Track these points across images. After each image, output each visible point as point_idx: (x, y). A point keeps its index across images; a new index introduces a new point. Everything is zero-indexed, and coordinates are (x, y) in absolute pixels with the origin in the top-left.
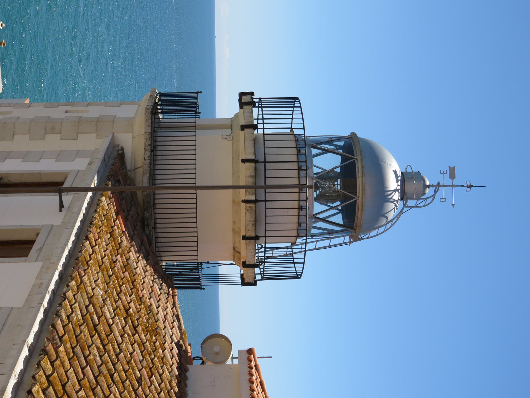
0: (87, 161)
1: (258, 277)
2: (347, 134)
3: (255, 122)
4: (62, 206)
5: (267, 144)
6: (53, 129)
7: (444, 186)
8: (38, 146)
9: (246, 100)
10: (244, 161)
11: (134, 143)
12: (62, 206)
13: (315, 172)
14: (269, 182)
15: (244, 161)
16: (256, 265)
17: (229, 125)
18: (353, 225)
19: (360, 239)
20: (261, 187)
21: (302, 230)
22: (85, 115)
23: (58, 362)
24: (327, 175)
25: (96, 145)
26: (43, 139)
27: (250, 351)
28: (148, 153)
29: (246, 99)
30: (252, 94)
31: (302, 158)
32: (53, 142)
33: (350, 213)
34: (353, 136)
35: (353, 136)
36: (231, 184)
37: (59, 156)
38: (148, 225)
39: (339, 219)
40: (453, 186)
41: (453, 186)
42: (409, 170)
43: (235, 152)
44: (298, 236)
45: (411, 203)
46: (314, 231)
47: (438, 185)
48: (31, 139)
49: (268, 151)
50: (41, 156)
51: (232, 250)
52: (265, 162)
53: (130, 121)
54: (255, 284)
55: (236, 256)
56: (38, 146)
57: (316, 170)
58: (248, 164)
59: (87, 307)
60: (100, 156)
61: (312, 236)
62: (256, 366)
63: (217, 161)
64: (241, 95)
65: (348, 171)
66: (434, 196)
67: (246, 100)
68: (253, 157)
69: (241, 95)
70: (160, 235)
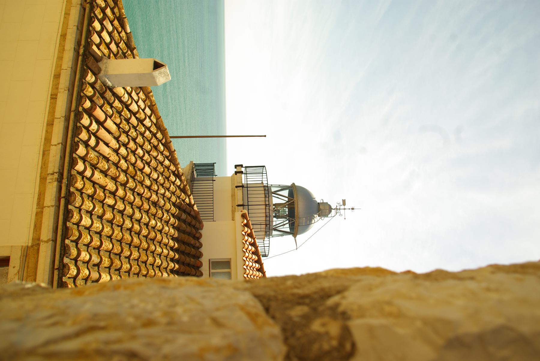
9: (239, 170)
10: (238, 206)
13: (274, 203)
18: (294, 230)
29: (239, 169)
30: (242, 166)
31: (267, 203)
39: (287, 228)
40: (345, 209)
41: (345, 209)
46: (274, 233)
52: (248, 205)
58: (239, 207)
65: (291, 205)
67: (239, 170)
69: (236, 166)
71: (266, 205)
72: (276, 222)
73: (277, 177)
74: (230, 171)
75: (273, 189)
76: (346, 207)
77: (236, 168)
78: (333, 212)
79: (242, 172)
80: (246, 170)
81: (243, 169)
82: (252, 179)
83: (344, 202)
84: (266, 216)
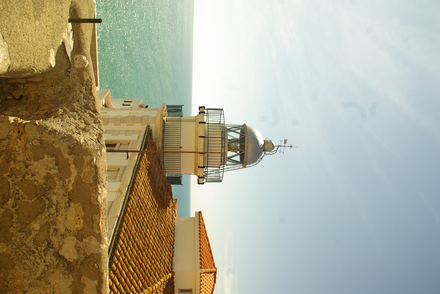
0: (137, 135)
1: (205, 180)
2: (242, 124)
3: (205, 121)
4: (128, 157)
5: (209, 130)
6: (124, 121)
7: (281, 146)
8: (117, 128)
10: (200, 137)
11: (156, 127)
12: (128, 157)
14: (209, 151)
15: (200, 137)
16: (203, 178)
17: (194, 120)
18: (243, 162)
19: (246, 167)
20: (206, 153)
21: (223, 163)
22: (136, 115)
23: (129, 224)
24: (235, 141)
25: (141, 128)
26: (120, 125)
27: (200, 213)
28: (161, 133)
30: (204, 107)
32: (124, 127)
33: (242, 157)
34: (244, 126)
35: (244, 126)
36: (194, 151)
37: (126, 133)
38: (161, 161)
39: (238, 158)
41: (285, 146)
42: (267, 139)
43: (197, 133)
44: (221, 165)
45: (267, 153)
46: (228, 163)
47: (279, 146)
48: (115, 125)
49: (209, 133)
50: (119, 132)
51: (194, 171)
53: (155, 118)
54: (203, 184)
55: (196, 173)
56: (117, 128)
57: (229, 138)
58: (201, 138)
59: (138, 201)
60: (143, 134)
61: (227, 165)
62: (202, 218)
63: (188, 138)
64: (200, 108)
65: (242, 140)
66: (276, 150)
68: (203, 135)
69: (200, 108)
70: (165, 165)
71: (222, 138)
72: (230, 154)
73: (231, 119)
74: (195, 112)
75: (228, 128)
76: (286, 145)
77: (199, 110)
78: (276, 148)
79: (204, 113)
80: (207, 111)
81: (205, 111)
82: (213, 119)
83: (285, 141)
84: (222, 147)
